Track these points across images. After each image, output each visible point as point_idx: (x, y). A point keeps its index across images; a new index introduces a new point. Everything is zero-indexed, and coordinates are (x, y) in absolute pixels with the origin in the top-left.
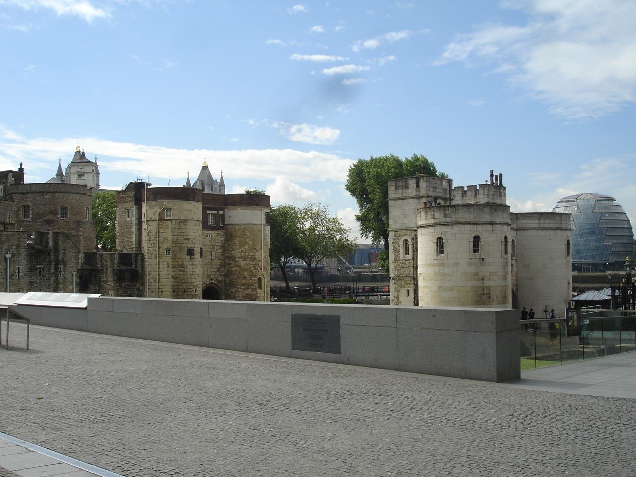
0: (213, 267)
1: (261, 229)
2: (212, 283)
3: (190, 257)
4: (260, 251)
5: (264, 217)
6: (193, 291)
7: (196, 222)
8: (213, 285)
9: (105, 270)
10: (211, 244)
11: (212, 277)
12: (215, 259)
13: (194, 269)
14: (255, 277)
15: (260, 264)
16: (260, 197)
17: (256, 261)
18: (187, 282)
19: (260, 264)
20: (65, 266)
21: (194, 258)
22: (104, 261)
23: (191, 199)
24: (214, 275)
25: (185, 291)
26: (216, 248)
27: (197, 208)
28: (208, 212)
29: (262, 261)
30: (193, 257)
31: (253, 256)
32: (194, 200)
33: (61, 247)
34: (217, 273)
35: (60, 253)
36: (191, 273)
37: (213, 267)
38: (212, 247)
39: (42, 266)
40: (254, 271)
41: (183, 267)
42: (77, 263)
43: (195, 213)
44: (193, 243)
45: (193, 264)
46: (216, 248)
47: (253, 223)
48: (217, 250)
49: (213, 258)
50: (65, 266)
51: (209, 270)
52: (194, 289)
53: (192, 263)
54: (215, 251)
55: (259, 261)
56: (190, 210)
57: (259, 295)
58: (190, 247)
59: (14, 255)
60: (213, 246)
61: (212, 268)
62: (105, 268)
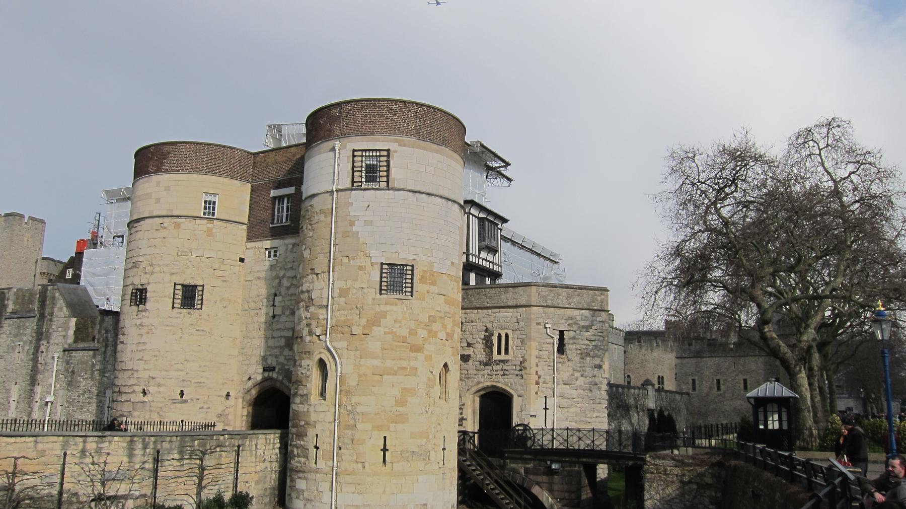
0: (277, 334)
2: (270, 379)
3: (135, 308)
6: (134, 392)
7: (161, 220)
8: (278, 385)
13: (142, 335)
15: (322, 313)
16: (335, 112)
19: (322, 313)
21: (145, 310)
23: (151, 169)
24: (276, 357)
26: (286, 283)
27: (167, 189)
32: (158, 171)
33: (47, 311)
34: (286, 352)
36: (134, 348)
37: (277, 334)
38: (277, 281)
39: (21, 343)
40: (308, 338)
43: (158, 201)
44: (146, 273)
45: (141, 325)
46: (286, 283)
47: (315, 192)
48: (288, 288)
49: (278, 311)
52: (139, 389)
53: (138, 322)
54: (283, 291)
55: (321, 307)
56: (149, 195)
57: (313, 417)
58: (137, 282)
61: (273, 337)
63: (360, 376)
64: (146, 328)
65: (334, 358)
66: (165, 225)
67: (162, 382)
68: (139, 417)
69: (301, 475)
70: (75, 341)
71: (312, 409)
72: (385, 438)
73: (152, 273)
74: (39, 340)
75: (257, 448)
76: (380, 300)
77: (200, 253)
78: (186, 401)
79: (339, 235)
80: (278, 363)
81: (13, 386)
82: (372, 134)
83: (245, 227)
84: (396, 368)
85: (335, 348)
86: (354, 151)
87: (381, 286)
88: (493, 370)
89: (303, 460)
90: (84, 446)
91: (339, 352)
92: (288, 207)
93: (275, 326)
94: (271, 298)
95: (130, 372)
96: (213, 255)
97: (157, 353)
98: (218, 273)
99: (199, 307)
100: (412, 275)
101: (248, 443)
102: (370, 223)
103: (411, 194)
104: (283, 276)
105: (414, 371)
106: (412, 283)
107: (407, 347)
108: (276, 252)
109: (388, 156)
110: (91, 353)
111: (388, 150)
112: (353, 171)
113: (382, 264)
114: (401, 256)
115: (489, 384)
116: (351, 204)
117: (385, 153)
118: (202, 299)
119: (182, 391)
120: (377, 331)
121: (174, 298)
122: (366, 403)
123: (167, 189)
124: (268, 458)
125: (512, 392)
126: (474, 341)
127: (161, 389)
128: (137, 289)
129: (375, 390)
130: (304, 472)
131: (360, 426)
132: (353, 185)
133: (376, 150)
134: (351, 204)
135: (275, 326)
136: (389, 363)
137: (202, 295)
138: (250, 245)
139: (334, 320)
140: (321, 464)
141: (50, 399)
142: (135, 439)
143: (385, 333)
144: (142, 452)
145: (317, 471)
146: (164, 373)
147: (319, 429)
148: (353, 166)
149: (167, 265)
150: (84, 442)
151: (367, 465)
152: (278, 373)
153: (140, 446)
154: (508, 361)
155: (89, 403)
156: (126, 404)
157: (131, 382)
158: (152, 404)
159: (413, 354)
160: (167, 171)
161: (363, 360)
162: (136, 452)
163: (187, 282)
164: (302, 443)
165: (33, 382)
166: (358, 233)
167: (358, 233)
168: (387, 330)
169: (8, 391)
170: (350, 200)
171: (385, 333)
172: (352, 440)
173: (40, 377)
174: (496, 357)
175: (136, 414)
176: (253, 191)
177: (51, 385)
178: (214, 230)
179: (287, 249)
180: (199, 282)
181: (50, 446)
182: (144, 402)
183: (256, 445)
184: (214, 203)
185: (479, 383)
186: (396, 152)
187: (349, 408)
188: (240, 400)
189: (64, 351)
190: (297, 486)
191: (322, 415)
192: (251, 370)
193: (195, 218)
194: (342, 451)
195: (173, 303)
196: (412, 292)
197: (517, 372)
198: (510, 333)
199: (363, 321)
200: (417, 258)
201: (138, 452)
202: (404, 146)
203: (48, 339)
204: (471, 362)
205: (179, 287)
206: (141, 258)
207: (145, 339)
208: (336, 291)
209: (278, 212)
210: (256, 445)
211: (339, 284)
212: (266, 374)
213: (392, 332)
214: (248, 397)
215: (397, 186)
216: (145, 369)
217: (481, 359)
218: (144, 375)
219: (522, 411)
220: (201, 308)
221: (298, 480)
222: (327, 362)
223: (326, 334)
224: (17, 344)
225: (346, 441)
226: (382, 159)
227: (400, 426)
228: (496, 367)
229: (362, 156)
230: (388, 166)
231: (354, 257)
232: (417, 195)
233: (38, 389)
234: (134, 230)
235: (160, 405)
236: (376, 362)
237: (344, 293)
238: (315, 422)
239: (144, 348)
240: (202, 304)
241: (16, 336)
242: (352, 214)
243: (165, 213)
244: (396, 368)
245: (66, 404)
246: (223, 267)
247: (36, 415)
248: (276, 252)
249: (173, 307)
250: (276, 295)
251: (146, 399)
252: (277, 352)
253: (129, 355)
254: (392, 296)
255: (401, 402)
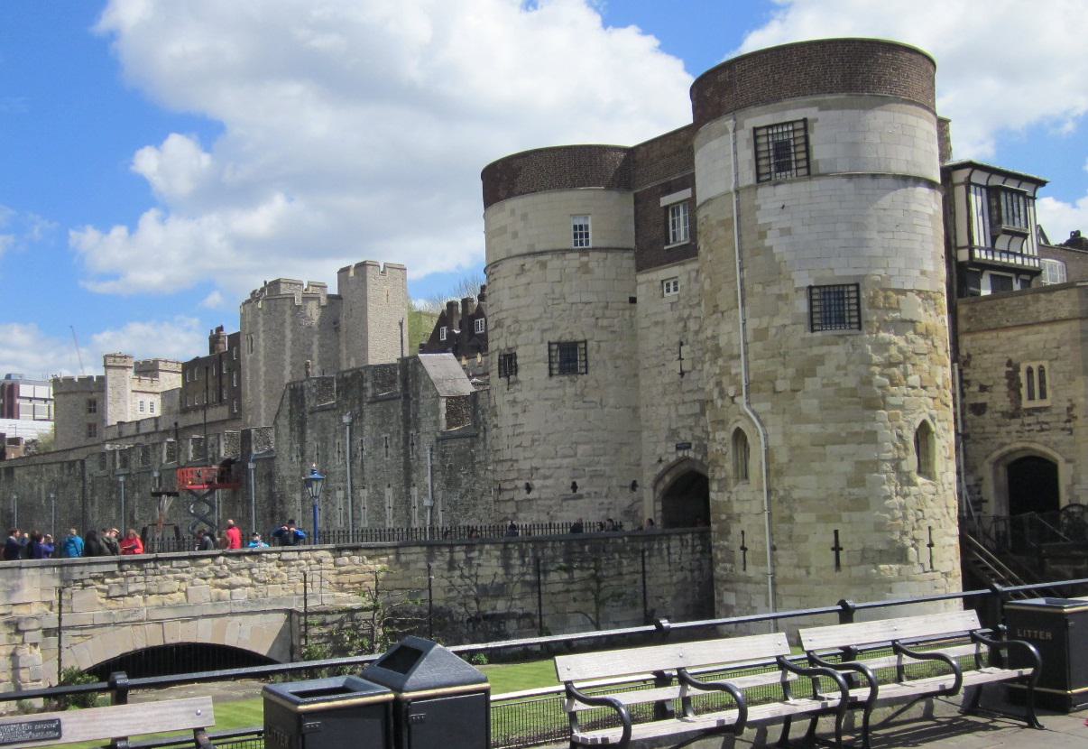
0: (688, 397)
1: (729, 216)
2: (687, 459)
3: (504, 380)
4: (733, 313)
5: (747, 154)
6: (516, 488)
7: (519, 262)
8: (697, 468)
9: (481, 435)
10: (676, 315)
11: (685, 436)
12: (694, 368)
13: (516, 415)
14: (723, 429)
16: (722, 77)
17: (720, 362)
18: (503, 461)
20: (418, 432)
21: (517, 382)
22: (480, 412)
23: (501, 194)
24: (691, 429)
25: (500, 490)
28: (665, 201)
29: (739, 356)
30: (512, 378)
31: (714, 337)
35: (411, 402)
37: (688, 397)
38: (681, 324)
40: (719, 403)
41: (496, 416)
42: (437, 423)
43: (515, 235)
44: (511, 334)
45: (514, 402)
46: (693, 325)
50: (418, 432)
51: (673, 415)
52: (521, 484)
53: (511, 398)
54: (690, 337)
57: (736, 508)
58: (503, 347)
59: (354, 418)
60: (685, 320)
61: (684, 403)
62: (482, 428)
63: (792, 449)
64: (519, 405)
65: (756, 427)
66: (527, 267)
67: (548, 473)
68: (525, 519)
69: (728, 586)
70: (450, 425)
71: (733, 497)
72: (836, 532)
73: (519, 333)
74: (407, 428)
75: (669, 553)
76: (812, 339)
77: (575, 298)
78: (581, 497)
79: (746, 255)
80: (694, 438)
81: (387, 489)
82: (779, 99)
83: (631, 254)
84: (843, 434)
85: (753, 412)
86: (755, 129)
87: (812, 319)
88: (1023, 424)
89: (729, 566)
90: (452, 557)
91: (761, 417)
92: (685, 218)
93: (686, 387)
94: (676, 348)
95: (510, 463)
96: (593, 298)
97: (536, 437)
98: (605, 322)
99: (583, 370)
100: (858, 298)
101: (656, 546)
102: (786, 232)
103: (844, 180)
104: (688, 318)
105: (872, 438)
106: (859, 310)
107: (858, 403)
108: (675, 283)
109: (806, 129)
110: (468, 441)
111: (805, 120)
112: (757, 160)
113: (811, 288)
114: (837, 273)
115: (1019, 445)
116: (758, 208)
117: (801, 125)
118: (586, 360)
119: (574, 484)
120: (811, 384)
121: (550, 362)
122: (805, 485)
123: (524, 217)
124: (687, 565)
125: (1057, 456)
126: (990, 383)
127: (549, 482)
128: (505, 356)
129: (816, 466)
130: (731, 582)
131: (800, 517)
132: (758, 181)
133: (782, 124)
134: (758, 208)
135: (686, 387)
136: (831, 429)
137: (586, 355)
138: (642, 278)
139: (751, 374)
140: (752, 571)
141: (427, 502)
142: (510, 546)
143: (824, 386)
144: (519, 562)
145: (748, 580)
146: (549, 462)
147: (745, 523)
148: (757, 153)
149: (535, 321)
150: (452, 552)
151: (813, 570)
152: (695, 451)
153: (516, 554)
154: (1045, 409)
155: (474, 506)
156: (510, 504)
157: (512, 475)
158: (539, 502)
159: (867, 413)
160: (521, 193)
161: (794, 428)
162: (513, 562)
163: (563, 339)
164: (726, 543)
165: (408, 483)
166: (771, 248)
167: (771, 248)
168: (825, 381)
169: (381, 495)
170: (757, 203)
171: (824, 386)
172: (790, 537)
173: (414, 476)
174: (1026, 404)
175: (521, 515)
176: (636, 202)
177: (427, 486)
178: (592, 265)
179: (689, 279)
180: (580, 338)
181: (413, 557)
182: (529, 500)
183: (668, 548)
184: (587, 227)
185: (1003, 445)
186: (816, 120)
187: (781, 493)
188: (651, 491)
189: (438, 440)
190: (725, 602)
191: (747, 506)
192: (660, 450)
193: (565, 251)
194: (779, 552)
195: (551, 369)
196: (859, 323)
197: (1062, 425)
198: (1045, 364)
199: (791, 371)
200: (861, 272)
201: (516, 562)
202: (828, 108)
203: (417, 426)
204: (987, 415)
205: (555, 347)
206: (504, 315)
207: (521, 419)
208: (749, 333)
209: (674, 228)
210: (668, 548)
211: (753, 323)
212: (680, 454)
213: (836, 384)
214: (661, 486)
215: (821, 171)
216: (525, 459)
217: (1005, 409)
218: (526, 465)
219: (1074, 484)
220: (586, 373)
221: (725, 593)
222: (747, 433)
223: (741, 394)
224: (384, 436)
225: (782, 538)
226: (797, 134)
227: (856, 516)
228: (1028, 420)
229: (768, 135)
230: (807, 143)
231: (766, 284)
232: (855, 180)
233: (415, 491)
234: (492, 278)
235: (548, 502)
236: (812, 428)
237: (761, 334)
238: (739, 515)
239: (521, 430)
240: (586, 366)
241: (381, 426)
242: (760, 222)
243: (525, 250)
244: (843, 434)
245: (448, 508)
246: (608, 313)
247: (416, 525)
248: (675, 283)
249: (551, 375)
250: (681, 344)
251: (531, 496)
252: (690, 421)
253: (505, 440)
254: (829, 333)
255: (857, 480)
